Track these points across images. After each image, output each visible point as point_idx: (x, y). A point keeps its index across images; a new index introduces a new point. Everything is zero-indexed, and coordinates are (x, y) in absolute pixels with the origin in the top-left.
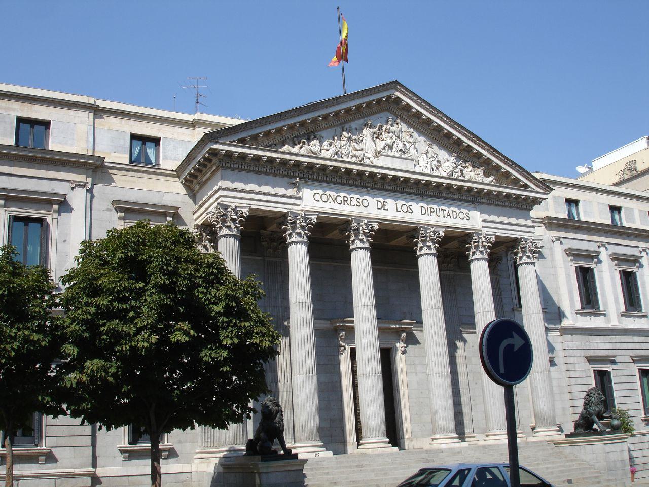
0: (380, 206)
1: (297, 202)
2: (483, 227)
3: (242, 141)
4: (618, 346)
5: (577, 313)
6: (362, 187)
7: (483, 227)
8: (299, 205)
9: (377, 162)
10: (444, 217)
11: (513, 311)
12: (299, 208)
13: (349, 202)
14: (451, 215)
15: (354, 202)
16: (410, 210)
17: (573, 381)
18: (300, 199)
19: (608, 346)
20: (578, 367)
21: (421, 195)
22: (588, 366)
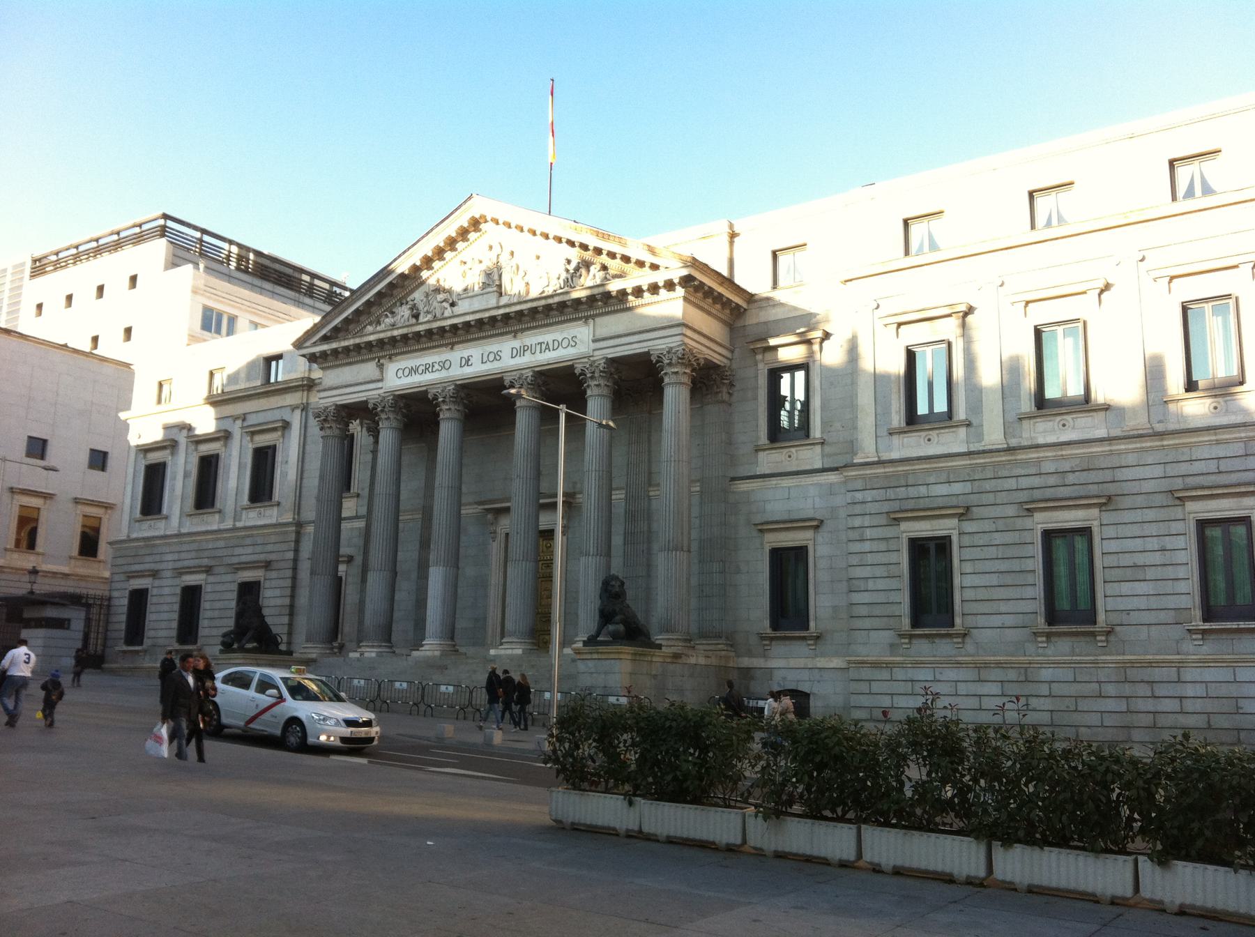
0: (463, 360)
1: (380, 385)
2: (594, 350)
3: (325, 339)
4: (988, 486)
5: (890, 434)
6: (446, 345)
8: (382, 388)
9: (458, 310)
10: (541, 352)
11: (757, 451)
12: (381, 391)
13: (430, 369)
14: (551, 348)
15: (437, 367)
16: (497, 356)
17: (854, 560)
18: (381, 380)
19: (957, 488)
20: (869, 533)
22: (889, 532)
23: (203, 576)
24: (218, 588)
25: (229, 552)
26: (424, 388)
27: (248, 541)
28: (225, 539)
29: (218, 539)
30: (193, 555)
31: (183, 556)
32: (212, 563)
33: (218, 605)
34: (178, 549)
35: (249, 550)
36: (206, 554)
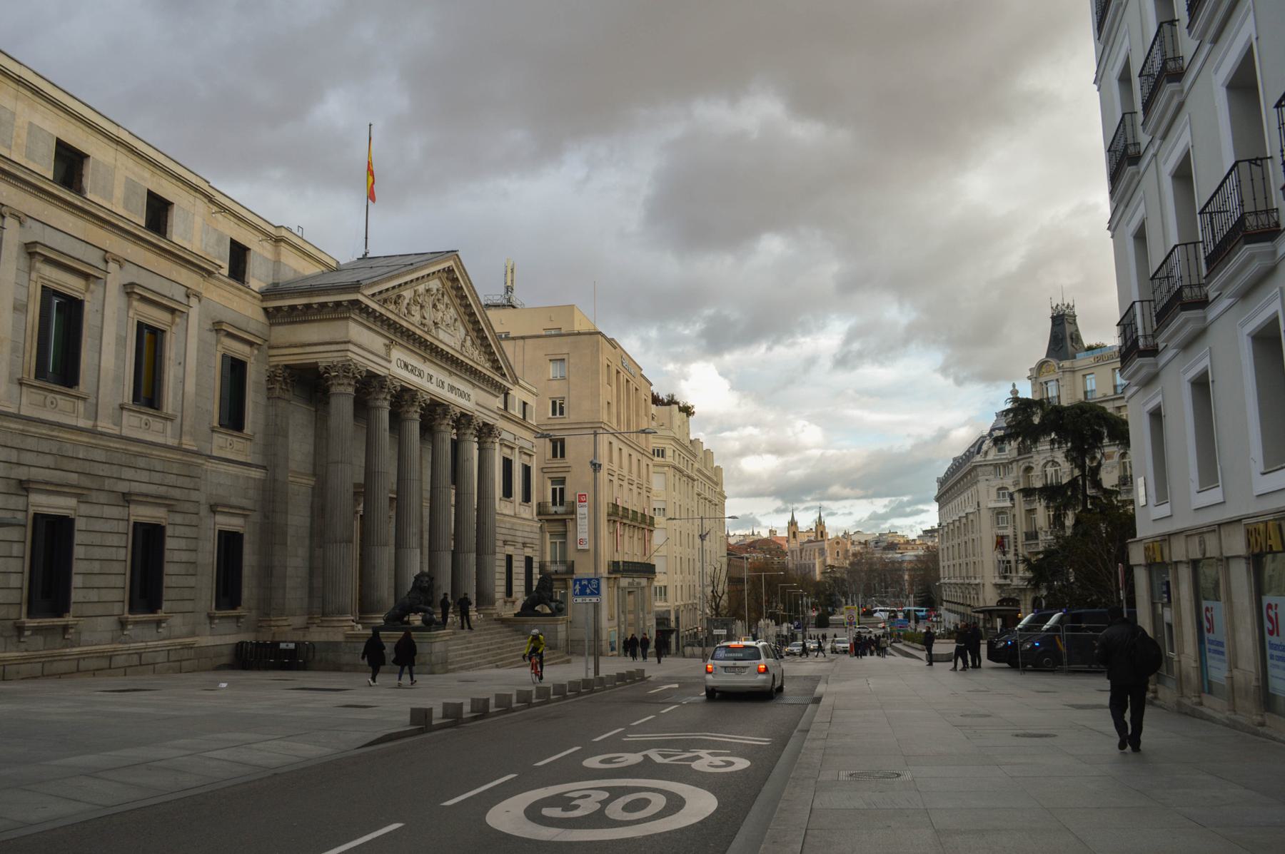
2: (477, 410)
7: (477, 410)
8: (389, 369)
21: (450, 372)
23: (72, 502)
24: (99, 525)
25: (115, 471)
26: (415, 389)
27: (141, 462)
28: (107, 449)
29: (95, 447)
30: (49, 460)
31: (28, 458)
32: (86, 482)
33: (98, 553)
34: (17, 442)
35: (144, 476)
36: (73, 465)
